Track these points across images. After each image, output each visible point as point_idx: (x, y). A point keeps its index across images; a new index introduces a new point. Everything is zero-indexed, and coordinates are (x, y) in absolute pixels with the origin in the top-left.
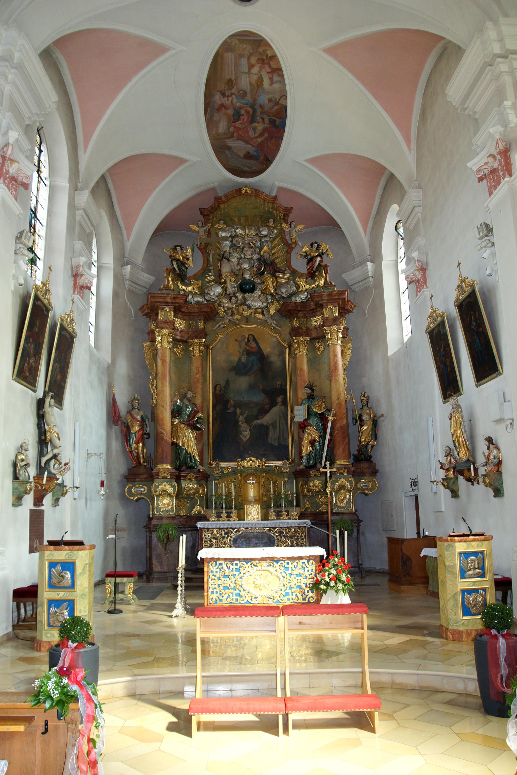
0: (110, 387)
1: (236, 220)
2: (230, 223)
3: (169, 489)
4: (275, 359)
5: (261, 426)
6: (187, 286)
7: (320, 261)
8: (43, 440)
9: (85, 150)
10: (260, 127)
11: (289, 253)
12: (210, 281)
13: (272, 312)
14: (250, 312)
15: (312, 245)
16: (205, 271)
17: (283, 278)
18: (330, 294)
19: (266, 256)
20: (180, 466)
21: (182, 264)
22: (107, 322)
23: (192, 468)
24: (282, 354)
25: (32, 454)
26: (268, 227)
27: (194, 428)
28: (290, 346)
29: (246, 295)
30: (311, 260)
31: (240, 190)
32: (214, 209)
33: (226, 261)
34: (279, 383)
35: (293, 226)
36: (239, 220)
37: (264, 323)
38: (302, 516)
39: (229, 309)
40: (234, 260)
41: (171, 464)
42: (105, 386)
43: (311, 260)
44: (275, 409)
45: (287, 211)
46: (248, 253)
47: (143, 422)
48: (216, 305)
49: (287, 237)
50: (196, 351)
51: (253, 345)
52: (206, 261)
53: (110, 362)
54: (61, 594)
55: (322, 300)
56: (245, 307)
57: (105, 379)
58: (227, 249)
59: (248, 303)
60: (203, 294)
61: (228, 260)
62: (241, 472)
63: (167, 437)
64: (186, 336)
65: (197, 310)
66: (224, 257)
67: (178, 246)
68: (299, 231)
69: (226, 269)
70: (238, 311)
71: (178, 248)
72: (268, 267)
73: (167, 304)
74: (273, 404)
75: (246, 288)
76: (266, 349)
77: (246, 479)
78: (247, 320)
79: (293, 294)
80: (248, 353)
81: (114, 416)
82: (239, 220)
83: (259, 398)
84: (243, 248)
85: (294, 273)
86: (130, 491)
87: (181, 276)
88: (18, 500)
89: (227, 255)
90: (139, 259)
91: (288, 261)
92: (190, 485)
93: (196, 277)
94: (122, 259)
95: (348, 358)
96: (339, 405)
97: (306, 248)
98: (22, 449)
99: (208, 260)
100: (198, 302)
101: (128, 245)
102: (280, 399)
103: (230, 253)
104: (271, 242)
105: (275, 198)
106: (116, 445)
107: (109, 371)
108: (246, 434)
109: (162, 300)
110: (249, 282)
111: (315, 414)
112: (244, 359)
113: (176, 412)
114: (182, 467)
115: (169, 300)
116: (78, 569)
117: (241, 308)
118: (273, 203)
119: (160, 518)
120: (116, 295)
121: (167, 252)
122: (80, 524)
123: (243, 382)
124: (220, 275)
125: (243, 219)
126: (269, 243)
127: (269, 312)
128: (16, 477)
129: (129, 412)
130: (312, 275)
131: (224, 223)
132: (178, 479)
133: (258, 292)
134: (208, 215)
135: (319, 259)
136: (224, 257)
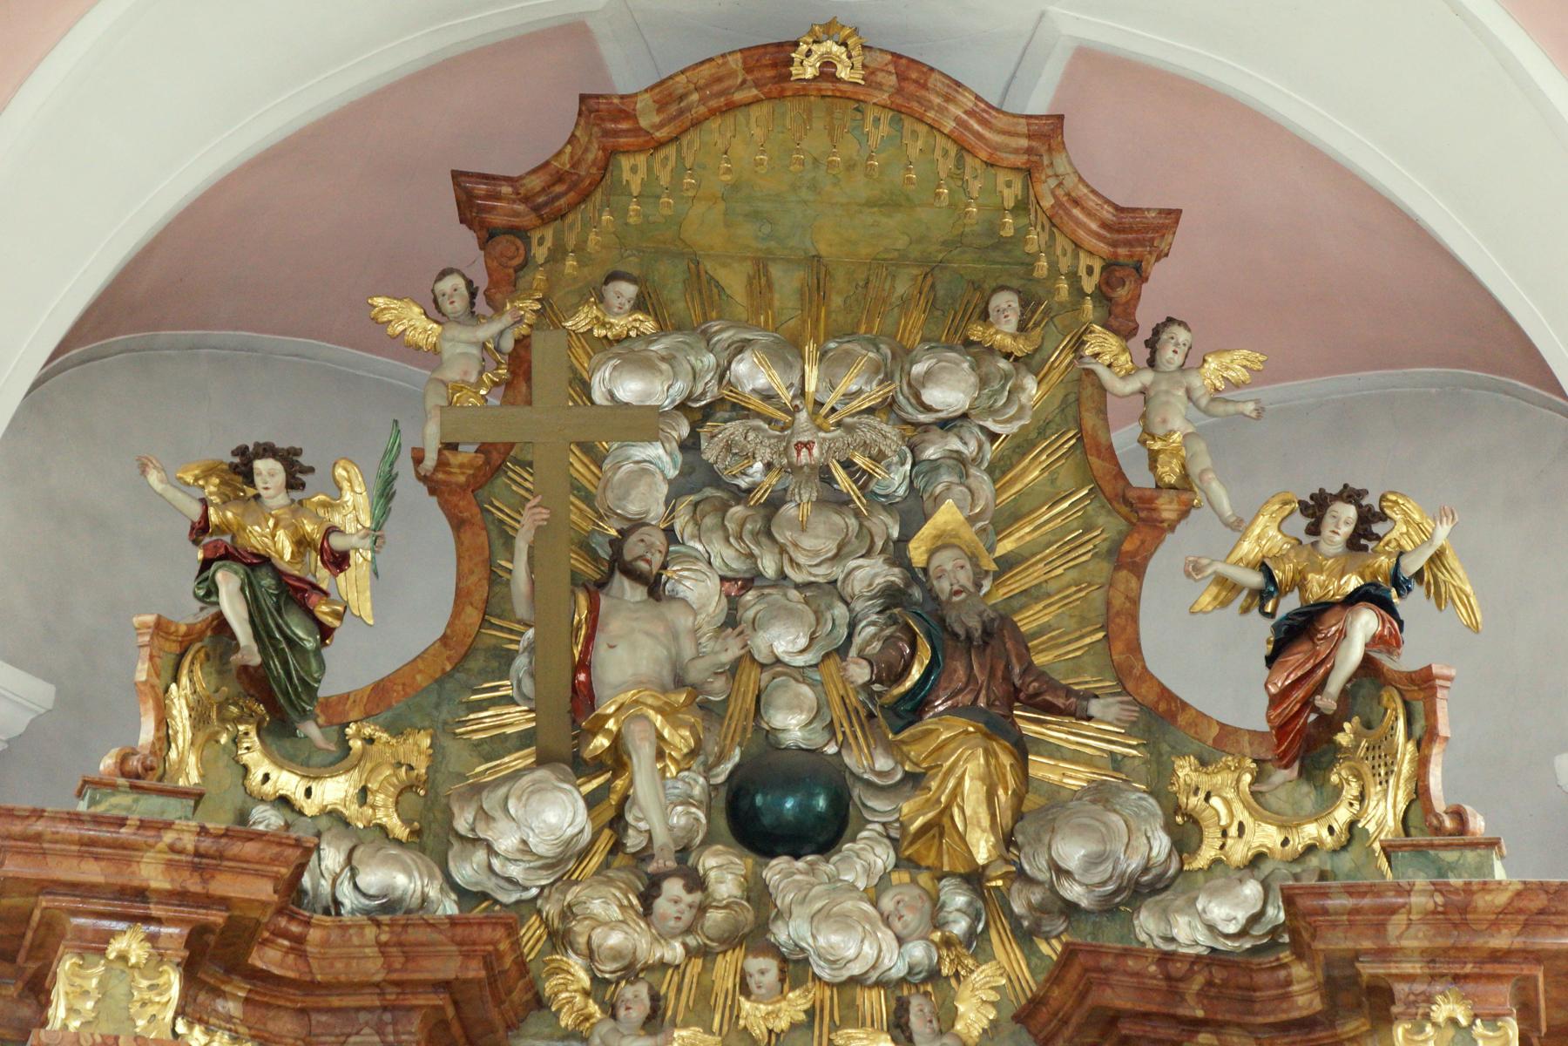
1: (734, 280)
2: (681, 297)
6: (314, 767)
7: (1376, 641)
11: (1128, 563)
12: (497, 746)
13: (973, 1015)
14: (795, 1005)
15: (1316, 509)
16: (467, 658)
17: (1069, 756)
18: (1456, 911)
19: (951, 574)
21: (286, 595)
26: (979, 352)
29: (778, 870)
30: (1301, 629)
31: (779, 55)
32: (567, 189)
33: (633, 593)
35: (1170, 356)
36: (760, 286)
39: (631, 971)
40: (698, 588)
43: (1301, 629)
45: (1137, 240)
46: (812, 540)
48: (532, 932)
49: (1124, 439)
52: (483, 591)
55: (1384, 954)
56: (764, 969)
58: (648, 501)
59: (781, 934)
60: (432, 837)
61: (654, 587)
65: (373, 968)
66: (617, 565)
67: (267, 451)
68: (1216, 395)
69: (629, 654)
70: (705, 994)
71: (268, 471)
72: (960, 658)
73: (132, 903)
75: (779, 812)
79: (1143, 888)
82: (760, 286)
84: (774, 504)
85: (1161, 718)
87: (275, 696)
89: (645, 549)
91: (1118, 627)
93: (389, 702)
97: (1267, 535)
99: (496, 579)
100: (389, 907)
103: (669, 532)
104: (997, 470)
105: (1048, 131)
109: (92, 872)
110: (809, 770)
115: (151, 873)
117: (725, 970)
118: (1028, 173)
121: (177, 491)
124: (582, 699)
125: (787, 283)
126: (980, 479)
127: (945, 1018)
130: (1303, 745)
131: (640, 305)
133: (867, 855)
134: (519, 233)
135: (1366, 622)
136: (619, 564)
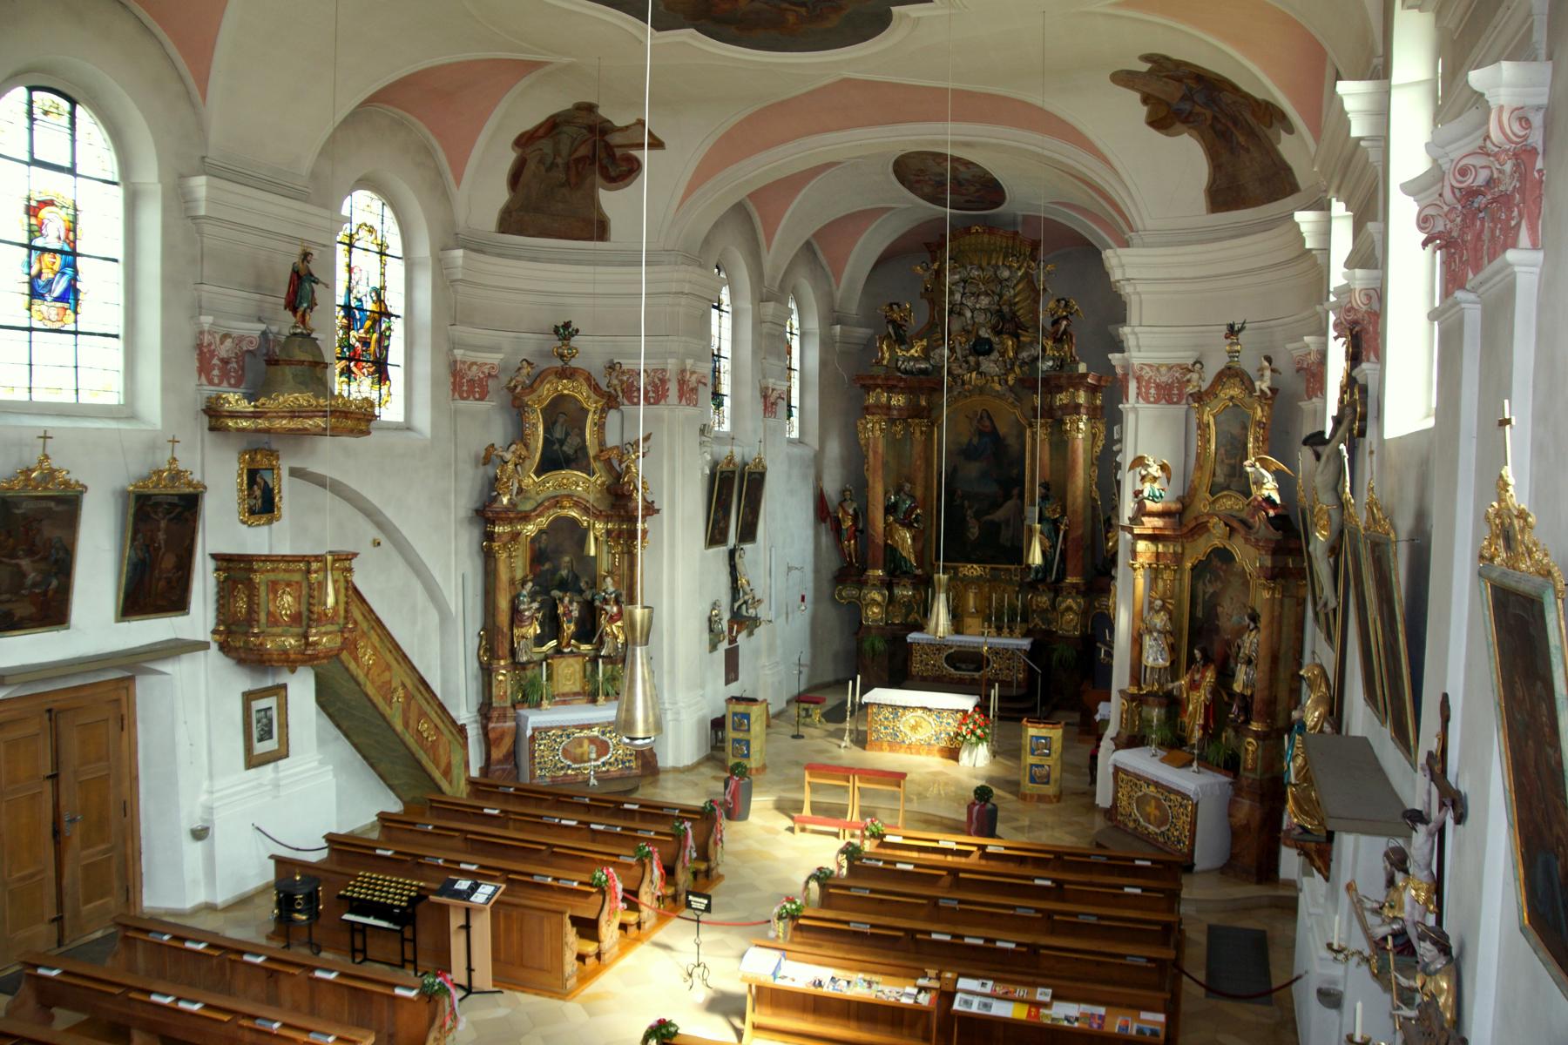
0: (818, 478)
3: (878, 598)
4: (1012, 441)
5: (992, 523)
8: (735, 589)
9: (769, 247)
10: (972, 189)
13: (1011, 382)
18: (1070, 377)
19: (1006, 309)
20: (895, 569)
21: (898, 327)
22: (813, 402)
23: (905, 573)
24: (1021, 435)
25: (725, 600)
26: (1010, 267)
27: (909, 526)
28: (1031, 426)
30: (1056, 323)
31: (967, 230)
34: (1015, 471)
37: (999, 396)
38: (1025, 635)
41: (884, 569)
42: (811, 480)
43: (1056, 323)
44: (1010, 504)
45: (1035, 245)
47: (855, 518)
50: (918, 434)
51: (987, 423)
53: (817, 447)
54: (740, 735)
57: (812, 472)
60: (927, 358)
62: (962, 580)
63: (880, 541)
64: (905, 414)
73: (878, 386)
74: (1007, 497)
75: (982, 348)
76: (1002, 429)
77: (966, 588)
78: (981, 390)
80: (981, 433)
81: (823, 511)
83: (992, 488)
86: (841, 597)
87: (901, 340)
88: (713, 647)
90: (853, 309)
92: (904, 592)
94: (833, 316)
95: (1100, 444)
96: (1075, 512)
98: (715, 605)
101: (838, 294)
102: (1015, 492)
106: (826, 540)
107: (818, 459)
108: (974, 531)
111: (1048, 519)
112: (975, 441)
113: (890, 509)
114: (895, 568)
116: (753, 719)
119: (869, 627)
120: (823, 364)
122: (778, 642)
123: (973, 469)
128: (711, 631)
129: (841, 504)
132: (889, 586)
